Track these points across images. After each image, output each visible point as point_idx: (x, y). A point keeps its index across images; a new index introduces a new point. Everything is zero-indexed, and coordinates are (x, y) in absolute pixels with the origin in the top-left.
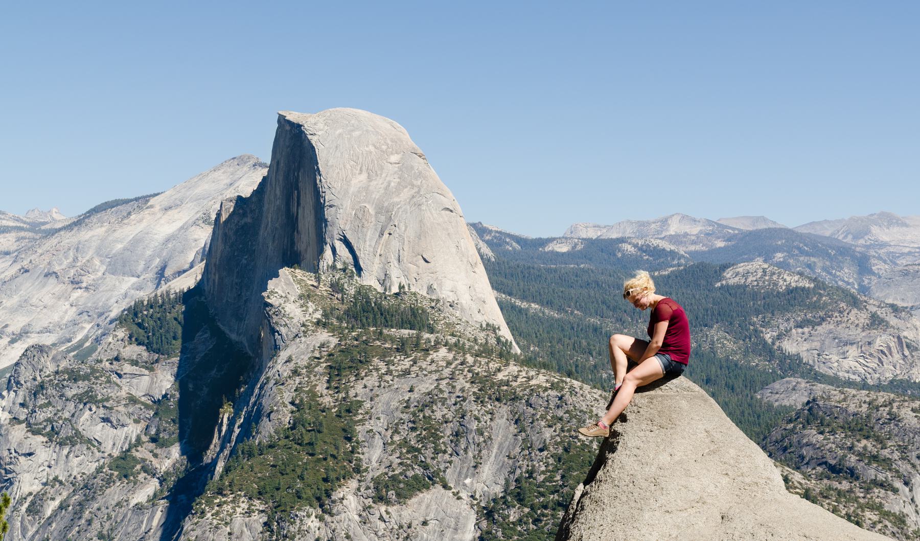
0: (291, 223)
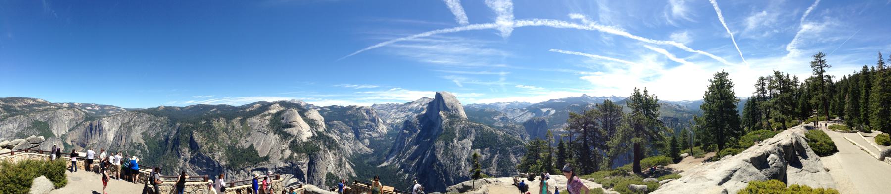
0: (438, 105)
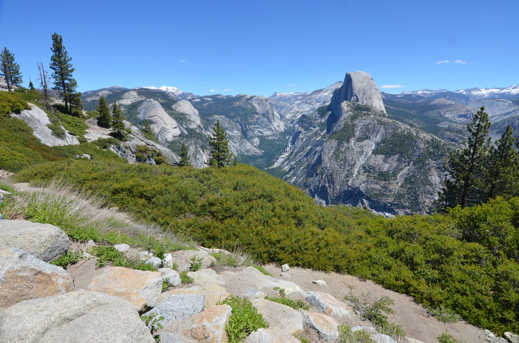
0: (347, 93)
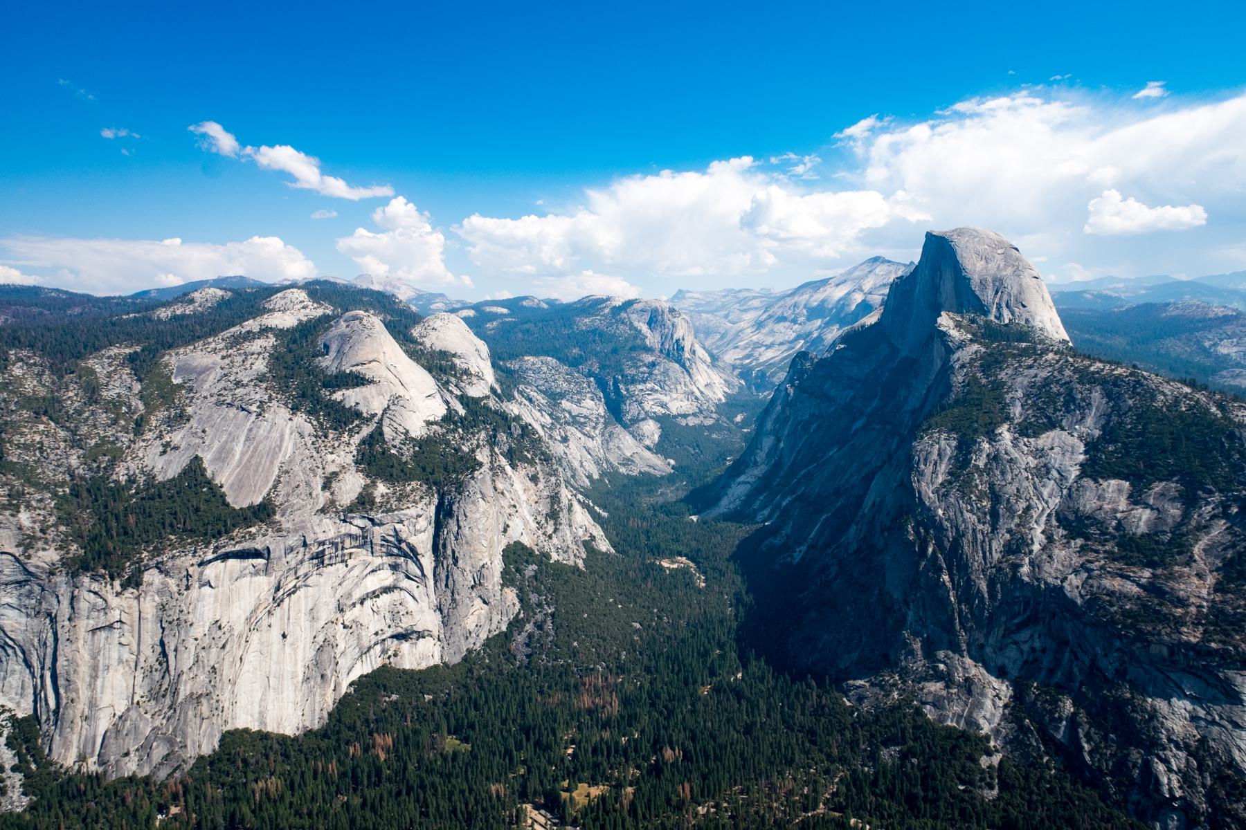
0: (936, 289)
